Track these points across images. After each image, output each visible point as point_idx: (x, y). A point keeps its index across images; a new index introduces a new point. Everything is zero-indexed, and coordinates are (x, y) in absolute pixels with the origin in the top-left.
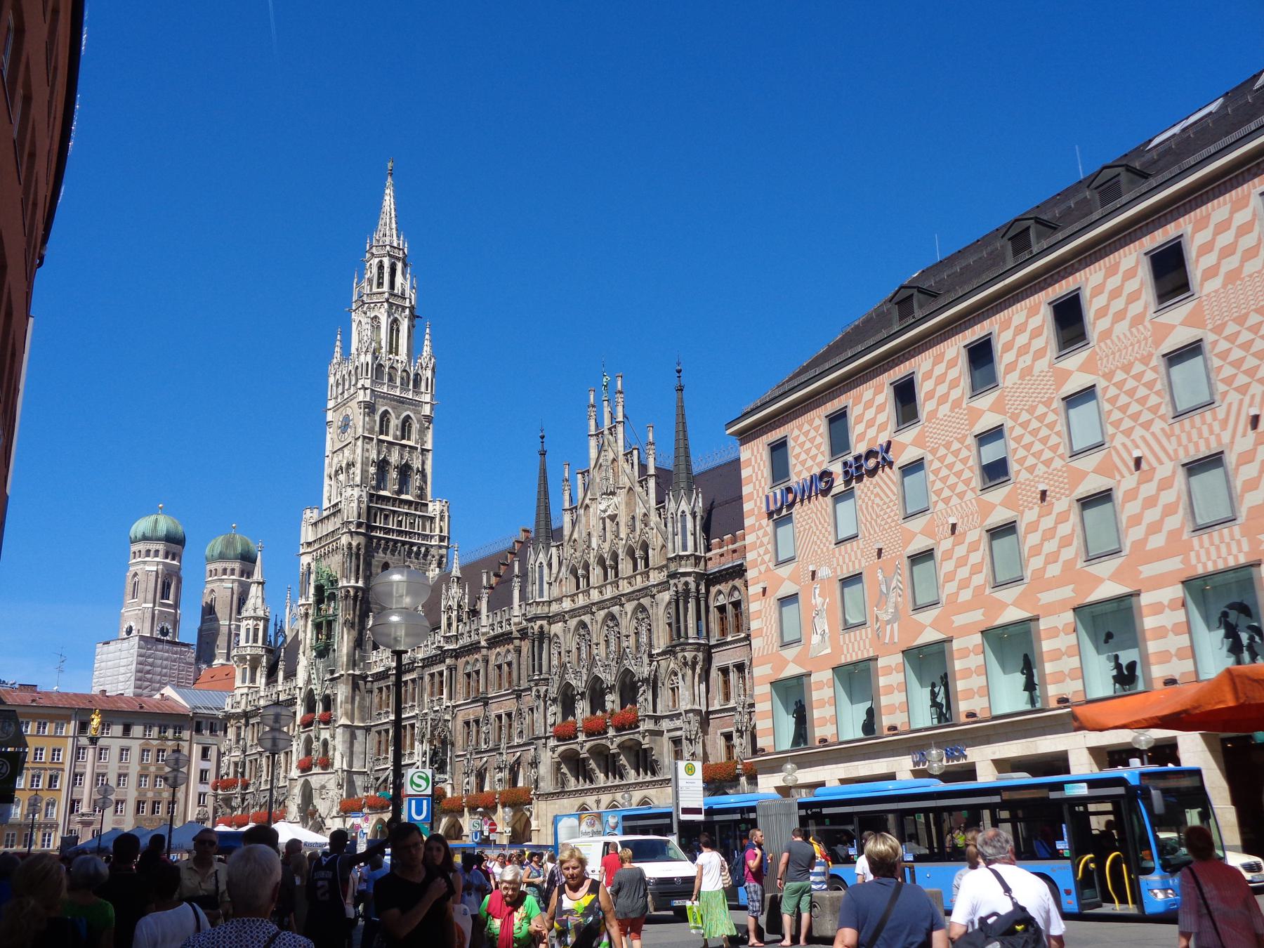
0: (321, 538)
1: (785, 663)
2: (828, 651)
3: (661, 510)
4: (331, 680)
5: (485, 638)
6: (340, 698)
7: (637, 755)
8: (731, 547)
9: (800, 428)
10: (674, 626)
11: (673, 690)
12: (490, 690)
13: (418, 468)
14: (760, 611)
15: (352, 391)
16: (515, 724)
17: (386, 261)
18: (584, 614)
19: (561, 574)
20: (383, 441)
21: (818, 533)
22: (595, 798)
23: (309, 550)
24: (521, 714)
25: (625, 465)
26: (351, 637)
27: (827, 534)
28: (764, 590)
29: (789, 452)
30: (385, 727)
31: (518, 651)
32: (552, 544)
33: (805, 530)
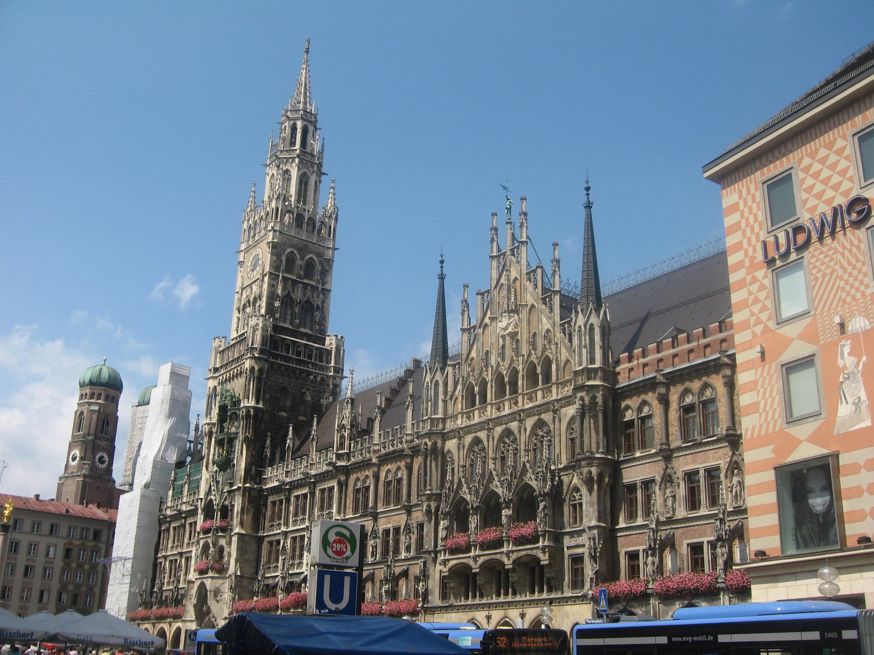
0: (227, 364)
1: (796, 443)
2: (868, 423)
3: (566, 326)
4: (229, 492)
5: (377, 455)
6: (237, 508)
8: (641, 361)
9: (813, 155)
11: (574, 506)
12: (379, 505)
13: (318, 305)
14: (755, 382)
15: (262, 234)
16: (403, 538)
17: (299, 124)
18: (480, 430)
19: (457, 392)
20: (288, 279)
21: (846, 276)
22: (485, 613)
23: (216, 375)
24: (409, 529)
25: (528, 283)
26: (249, 453)
28: (763, 353)
29: (795, 186)
30: (277, 538)
31: (410, 468)
32: (448, 363)
33: (824, 276)
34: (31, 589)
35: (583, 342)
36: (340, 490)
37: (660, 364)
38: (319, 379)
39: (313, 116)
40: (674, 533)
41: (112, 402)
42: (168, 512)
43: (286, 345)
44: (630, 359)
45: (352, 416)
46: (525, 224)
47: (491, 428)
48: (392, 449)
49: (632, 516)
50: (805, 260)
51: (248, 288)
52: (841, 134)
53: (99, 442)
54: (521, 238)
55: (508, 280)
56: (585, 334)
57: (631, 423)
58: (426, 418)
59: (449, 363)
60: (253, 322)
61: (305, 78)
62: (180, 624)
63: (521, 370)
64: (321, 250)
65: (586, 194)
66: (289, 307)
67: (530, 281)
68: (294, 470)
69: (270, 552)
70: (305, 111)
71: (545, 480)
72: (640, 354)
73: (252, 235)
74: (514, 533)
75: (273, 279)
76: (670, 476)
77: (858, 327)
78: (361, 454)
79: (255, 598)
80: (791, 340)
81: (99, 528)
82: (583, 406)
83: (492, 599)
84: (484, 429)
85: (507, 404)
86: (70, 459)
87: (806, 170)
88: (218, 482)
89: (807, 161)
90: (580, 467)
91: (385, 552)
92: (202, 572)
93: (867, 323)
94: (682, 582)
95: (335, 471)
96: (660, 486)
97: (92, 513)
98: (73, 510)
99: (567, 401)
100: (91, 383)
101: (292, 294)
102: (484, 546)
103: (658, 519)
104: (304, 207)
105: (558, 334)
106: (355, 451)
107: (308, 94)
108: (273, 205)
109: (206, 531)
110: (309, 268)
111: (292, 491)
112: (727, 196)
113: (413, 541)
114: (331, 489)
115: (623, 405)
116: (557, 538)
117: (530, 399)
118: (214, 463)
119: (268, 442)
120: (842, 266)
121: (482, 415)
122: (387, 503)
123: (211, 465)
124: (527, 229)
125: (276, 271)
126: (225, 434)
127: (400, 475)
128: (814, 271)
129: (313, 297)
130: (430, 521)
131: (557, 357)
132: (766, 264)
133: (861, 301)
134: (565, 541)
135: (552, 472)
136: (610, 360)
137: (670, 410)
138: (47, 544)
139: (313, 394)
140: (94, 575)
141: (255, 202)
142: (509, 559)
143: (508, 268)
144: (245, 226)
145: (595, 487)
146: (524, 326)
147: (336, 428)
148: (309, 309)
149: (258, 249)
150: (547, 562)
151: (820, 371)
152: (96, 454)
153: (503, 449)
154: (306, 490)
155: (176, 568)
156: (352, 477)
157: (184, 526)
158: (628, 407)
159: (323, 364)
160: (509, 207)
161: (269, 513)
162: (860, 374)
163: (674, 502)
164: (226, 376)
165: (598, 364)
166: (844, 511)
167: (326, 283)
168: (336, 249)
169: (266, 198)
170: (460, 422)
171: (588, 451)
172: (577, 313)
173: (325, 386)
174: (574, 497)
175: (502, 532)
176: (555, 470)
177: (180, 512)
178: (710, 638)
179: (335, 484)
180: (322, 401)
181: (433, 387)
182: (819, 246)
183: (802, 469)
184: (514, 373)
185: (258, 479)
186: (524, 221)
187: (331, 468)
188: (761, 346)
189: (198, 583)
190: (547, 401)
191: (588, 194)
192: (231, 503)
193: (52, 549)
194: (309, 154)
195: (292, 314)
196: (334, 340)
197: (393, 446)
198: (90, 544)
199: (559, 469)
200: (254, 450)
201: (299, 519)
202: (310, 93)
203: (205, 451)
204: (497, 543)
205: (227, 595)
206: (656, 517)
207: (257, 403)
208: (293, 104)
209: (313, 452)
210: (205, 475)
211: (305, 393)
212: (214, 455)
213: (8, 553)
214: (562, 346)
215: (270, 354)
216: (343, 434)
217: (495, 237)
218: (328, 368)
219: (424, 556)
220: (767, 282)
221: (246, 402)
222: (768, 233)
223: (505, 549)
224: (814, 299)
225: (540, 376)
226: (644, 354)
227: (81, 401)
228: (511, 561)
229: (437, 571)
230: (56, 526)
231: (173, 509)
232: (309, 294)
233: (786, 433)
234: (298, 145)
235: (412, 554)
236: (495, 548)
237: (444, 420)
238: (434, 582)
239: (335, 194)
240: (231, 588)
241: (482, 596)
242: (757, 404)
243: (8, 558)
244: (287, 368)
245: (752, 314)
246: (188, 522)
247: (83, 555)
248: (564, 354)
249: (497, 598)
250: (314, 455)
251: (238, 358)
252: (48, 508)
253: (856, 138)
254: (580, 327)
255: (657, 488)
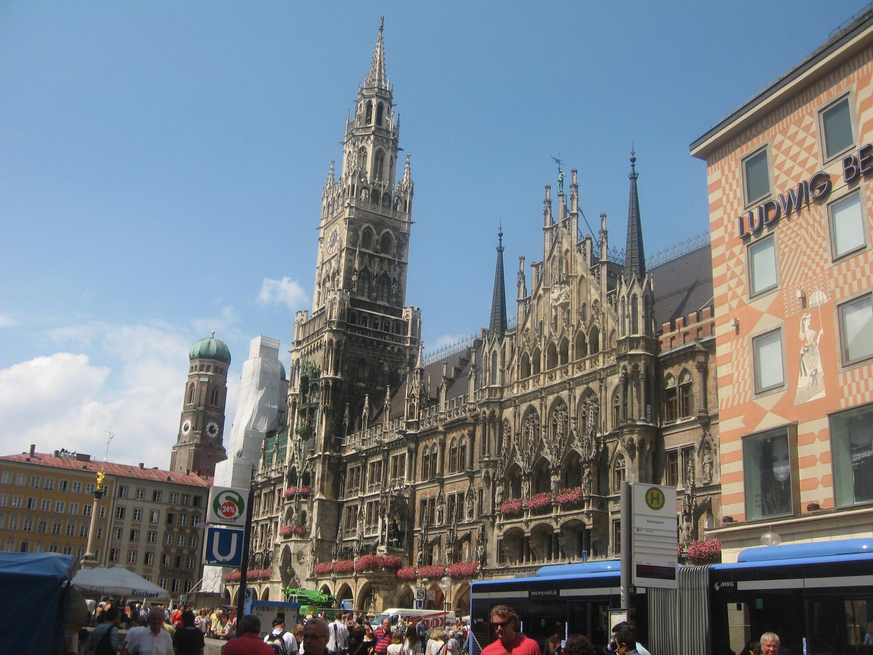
0: (308, 337)
1: (761, 413)
2: (822, 394)
3: (613, 296)
4: (311, 460)
5: (443, 423)
6: (318, 475)
7: (580, 537)
8: (683, 329)
9: (784, 132)
10: (621, 409)
11: (619, 472)
12: (446, 471)
14: (731, 354)
15: (340, 210)
16: (466, 503)
17: (374, 102)
18: (534, 399)
19: (514, 362)
20: (365, 253)
23: (299, 348)
24: (472, 495)
25: (578, 255)
26: (329, 423)
27: (821, 251)
30: (354, 503)
31: (472, 436)
33: (790, 251)
34: (137, 552)
35: (626, 312)
36: (410, 458)
37: (699, 333)
38: (396, 350)
39: (388, 93)
40: (711, 499)
41: (221, 373)
42: (260, 479)
43: (363, 317)
44: (673, 328)
45: (421, 386)
46: (576, 196)
47: (544, 397)
48: (457, 418)
49: (673, 482)
50: (775, 235)
51: (328, 264)
52: (809, 111)
53: (209, 413)
54: (572, 210)
55: (560, 252)
56: (628, 304)
57: (672, 391)
58: (484, 387)
59: (506, 333)
60: (331, 296)
61: (380, 56)
62: (268, 585)
63: (571, 340)
64: (397, 224)
65: (632, 165)
66: (366, 281)
67: (581, 253)
68: (370, 439)
69: (349, 517)
70: (380, 89)
71: (590, 447)
72: (681, 323)
73: (330, 212)
74: (561, 499)
75: (350, 254)
76: (708, 443)
77: (817, 301)
78: (429, 423)
79: (333, 561)
80: (760, 314)
81: (198, 494)
82: (626, 374)
83: (543, 562)
84: (538, 398)
85: (558, 372)
86: (183, 429)
87: (778, 147)
88: (300, 450)
89: (779, 138)
90: (622, 434)
91: (450, 518)
92: (287, 536)
93: (825, 297)
94: (714, 547)
95: (407, 439)
96: (699, 453)
97: (192, 481)
98: (175, 478)
99: (612, 370)
100: (201, 356)
101: (369, 268)
102: (535, 511)
103: (694, 485)
104: (380, 182)
105: (605, 305)
106: (424, 420)
107: (383, 71)
108: (349, 182)
109: (290, 497)
110: (386, 242)
111: (369, 459)
112: (712, 173)
113: (475, 506)
114: (403, 456)
115: (666, 373)
116: (602, 504)
117: (580, 368)
118: (297, 432)
119: (347, 412)
120: (806, 242)
121: (536, 384)
122: (453, 470)
123: (294, 434)
124: (578, 201)
125: (353, 246)
126: (307, 405)
127: (464, 443)
128: (782, 246)
129: (390, 271)
130: (488, 487)
131: (604, 327)
132: (742, 240)
133: (821, 275)
134: (609, 506)
135: (598, 440)
136: (653, 329)
137: (709, 378)
138: (151, 510)
139: (391, 365)
140: (195, 539)
141: (333, 180)
142: (557, 524)
143: (560, 239)
144: (325, 203)
145: (637, 453)
146: (574, 297)
147: (406, 397)
148: (386, 282)
149: (336, 226)
150: (591, 527)
151: (784, 344)
152: (207, 424)
153: (555, 417)
154: (379, 458)
155: (266, 531)
156: (421, 444)
157: (273, 492)
158: (670, 376)
159: (400, 335)
160: (561, 179)
161: (348, 480)
162: (817, 347)
163: (711, 469)
164: (308, 348)
165: (640, 334)
166: (800, 479)
167: (402, 256)
168: (412, 223)
169: (344, 176)
170: (516, 391)
171: (630, 419)
172: (621, 284)
173: (402, 357)
174: (619, 464)
175: (551, 498)
176: (601, 437)
177: (270, 479)
178: (555, 593)
179: (406, 452)
180: (399, 371)
181: (491, 357)
182: (787, 221)
183: (767, 439)
184: (565, 342)
185: (337, 447)
186: (575, 194)
187: (402, 436)
188: (735, 320)
189: (283, 547)
190: (594, 370)
191: (633, 166)
192: (312, 470)
193: (155, 515)
194: (384, 130)
195: (369, 287)
196: (411, 312)
197: (457, 414)
198: (191, 510)
199: (604, 437)
200: (333, 420)
201: (374, 485)
202: (385, 70)
203: (289, 421)
204: (547, 509)
205: (309, 558)
206: (692, 483)
207: (336, 374)
208: (368, 82)
209: (386, 421)
210: (290, 444)
211: (382, 363)
212: (297, 425)
213: (115, 518)
214: (609, 316)
215: (348, 327)
216: (413, 404)
217: (548, 209)
218: (405, 339)
219: (483, 520)
220: (743, 257)
221: (325, 374)
222: (745, 209)
223: (553, 514)
224: (782, 275)
225: (588, 346)
226: (685, 324)
227: (192, 373)
228: (559, 526)
229: (495, 536)
230: (159, 494)
231: (263, 476)
232: (386, 267)
233: (755, 403)
234: (373, 123)
235: (474, 519)
236: (545, 513)
237: (502, 389)
238: (492, 546)
239: (410, 169)
240: (312, 551)
241: (534, 560)
242: (731, 375)
243: (115, 523)
244: (364, 340)
245: (730, 288)
246: (277, 488)
247: (184, 520)
248: (611, 324)
249: (548, 561)
250: (387, 423)
251: (318, 331)
252: (152, 476)
253: (821, 114)
254: (623, 297)
255: (696, 454)
